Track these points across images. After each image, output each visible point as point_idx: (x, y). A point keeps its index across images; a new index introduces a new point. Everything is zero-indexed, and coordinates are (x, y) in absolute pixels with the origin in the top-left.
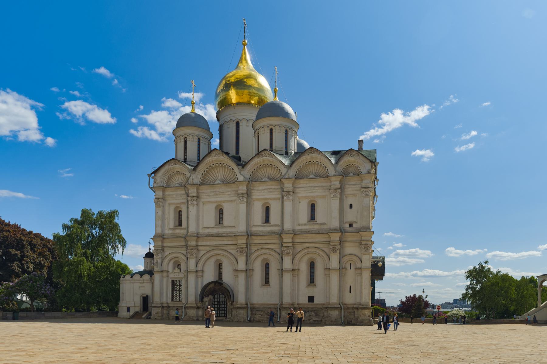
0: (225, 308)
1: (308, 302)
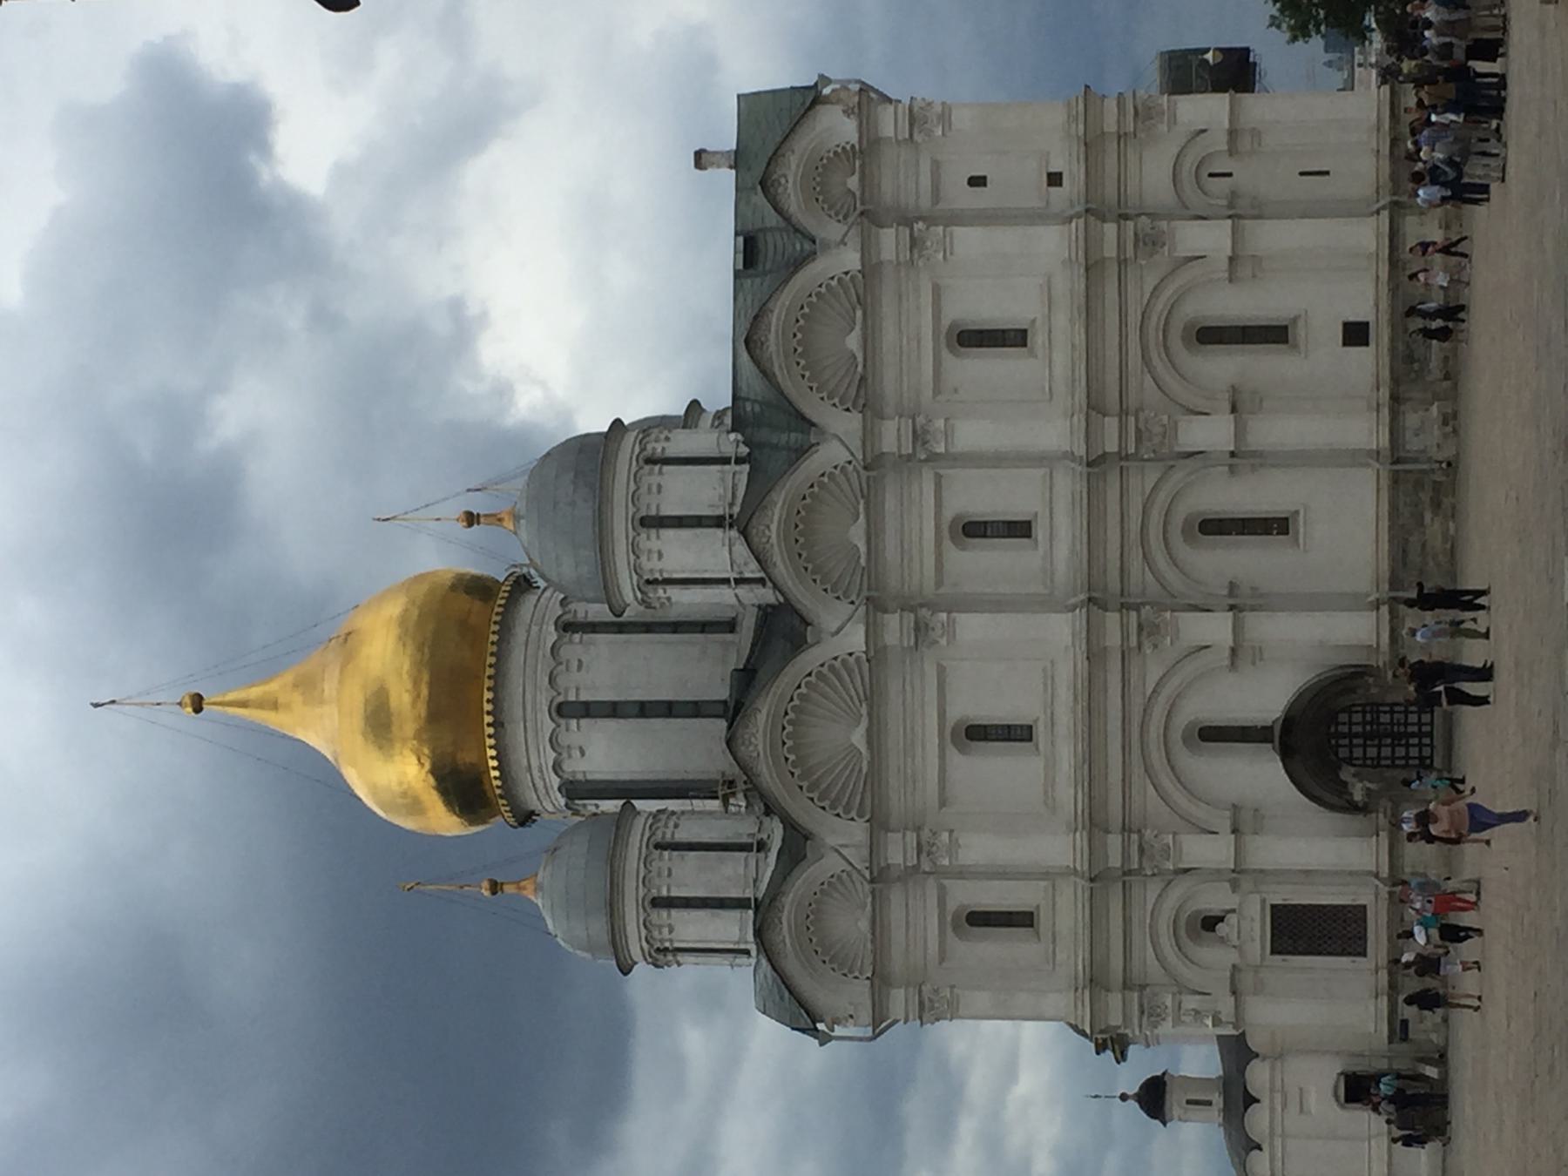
1: (1367, 344)
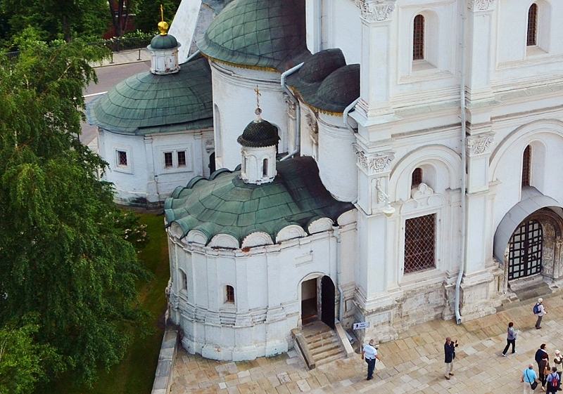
0: (540, 253)
